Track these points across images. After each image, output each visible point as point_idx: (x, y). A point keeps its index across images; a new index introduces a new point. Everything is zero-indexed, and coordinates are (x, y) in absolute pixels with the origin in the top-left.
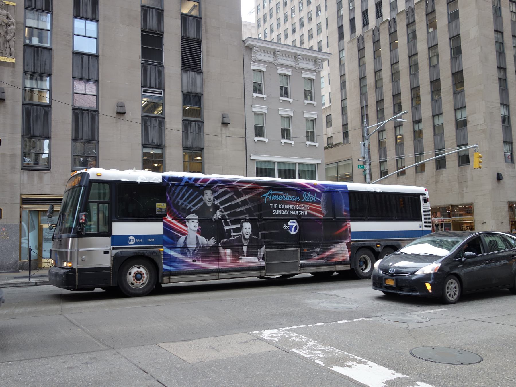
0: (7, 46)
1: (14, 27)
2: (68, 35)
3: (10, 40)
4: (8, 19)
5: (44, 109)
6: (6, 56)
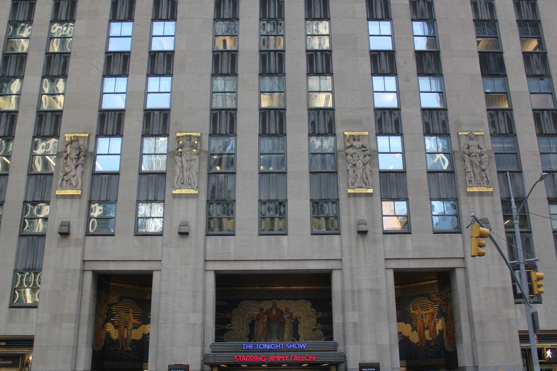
0: (484, 175)
1: (487, 156)
2: (536, 154)
3: (486, 169)
4: (479, 148)
5: (525, 236)
6: (484, 186)
